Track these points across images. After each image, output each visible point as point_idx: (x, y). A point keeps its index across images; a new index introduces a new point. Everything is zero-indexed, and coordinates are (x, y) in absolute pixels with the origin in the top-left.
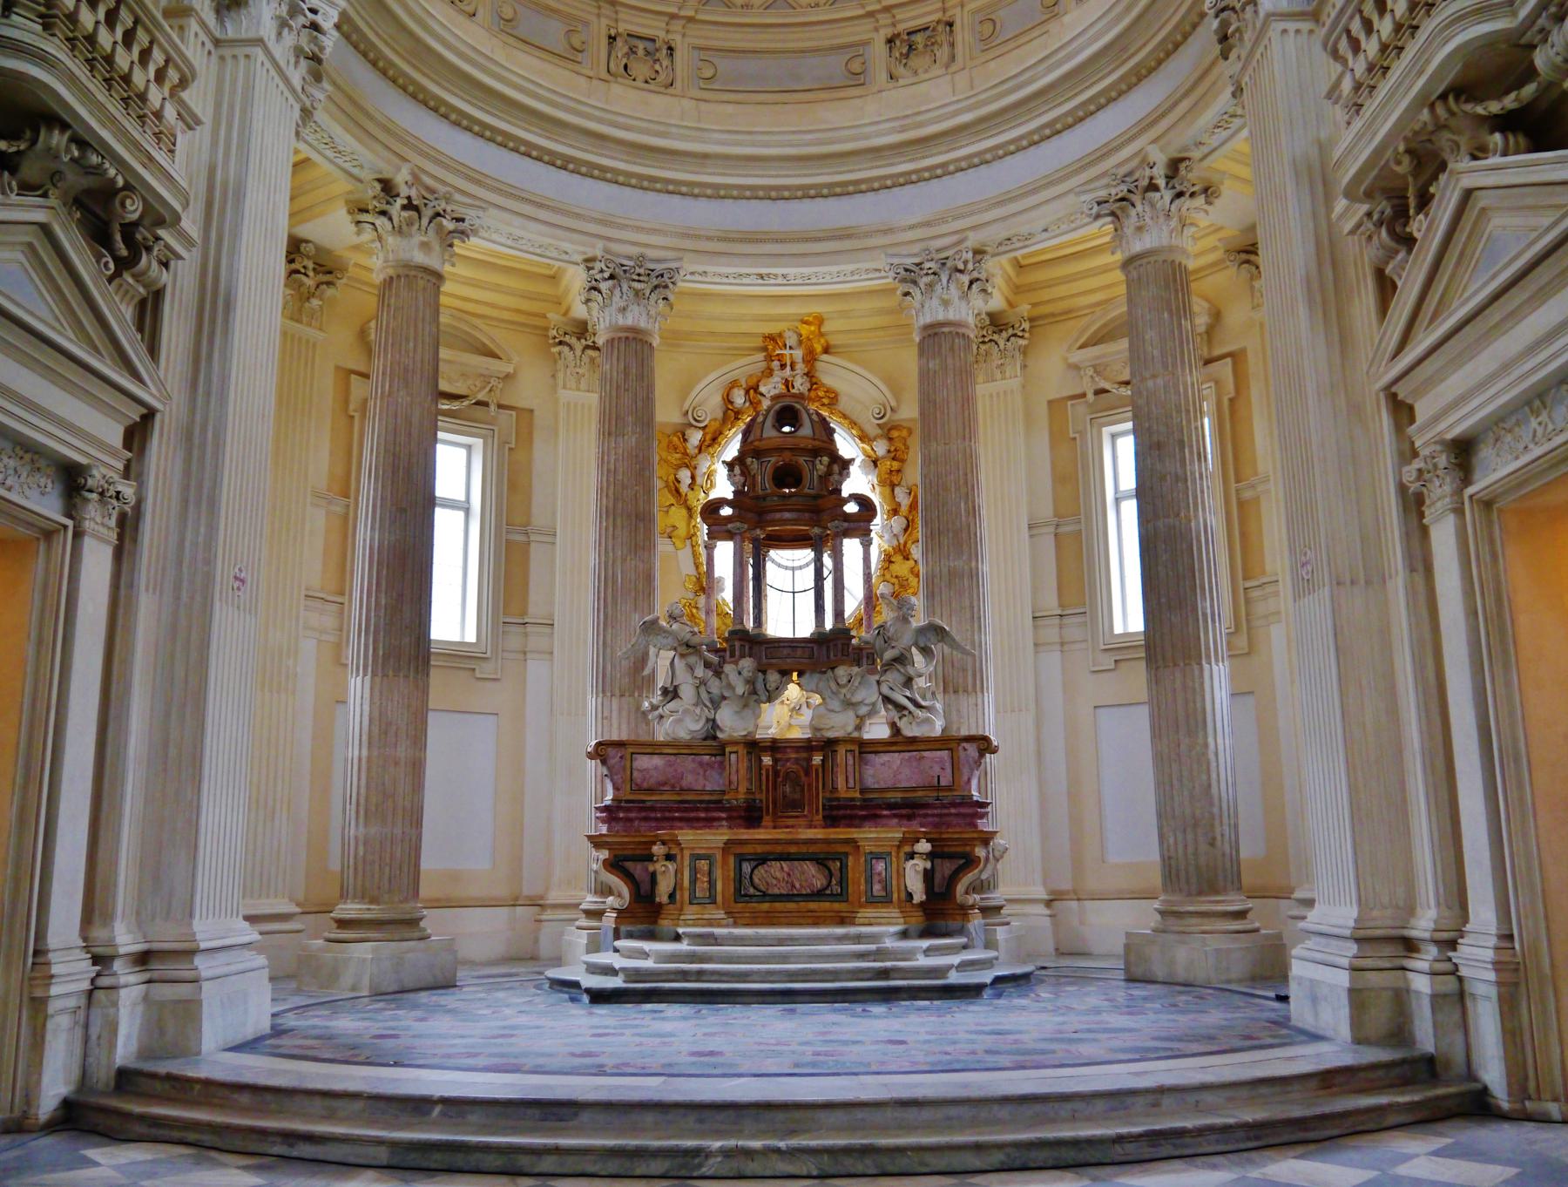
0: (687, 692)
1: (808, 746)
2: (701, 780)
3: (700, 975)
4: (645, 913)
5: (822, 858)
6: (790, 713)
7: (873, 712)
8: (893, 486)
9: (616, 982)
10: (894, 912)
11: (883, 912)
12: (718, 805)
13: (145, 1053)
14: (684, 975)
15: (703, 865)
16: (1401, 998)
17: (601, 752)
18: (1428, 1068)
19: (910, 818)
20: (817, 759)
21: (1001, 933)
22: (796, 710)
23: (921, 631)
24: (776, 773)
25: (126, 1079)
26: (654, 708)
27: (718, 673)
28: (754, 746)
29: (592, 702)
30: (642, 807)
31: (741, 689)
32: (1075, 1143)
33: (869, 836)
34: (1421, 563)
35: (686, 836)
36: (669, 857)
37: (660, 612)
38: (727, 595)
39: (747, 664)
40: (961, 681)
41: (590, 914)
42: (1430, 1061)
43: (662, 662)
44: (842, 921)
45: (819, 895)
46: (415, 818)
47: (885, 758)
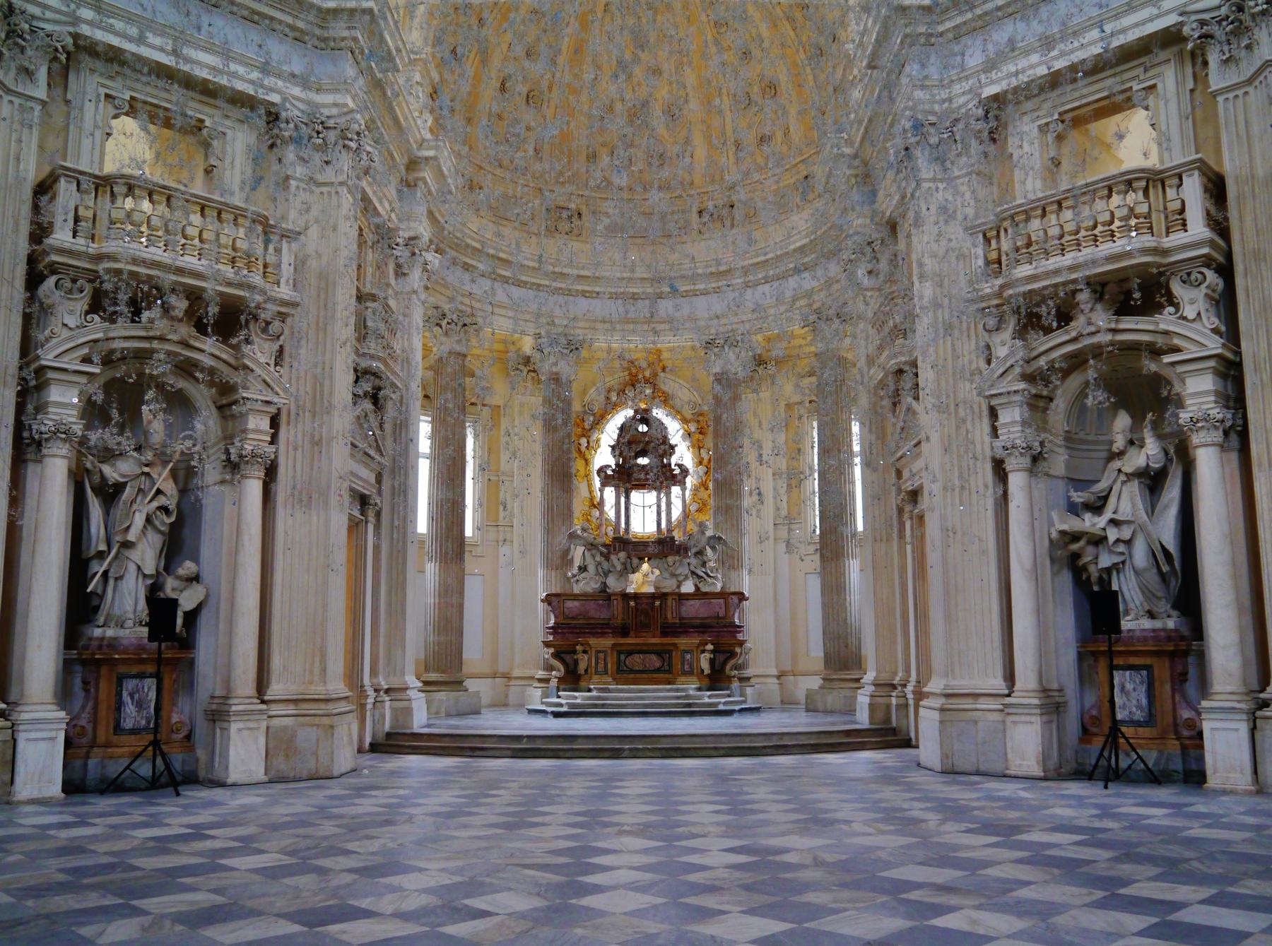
0: (591, 568)
1: (652, 597)
2: (599, 613)
3: (603, 706)
4: (572, 679)
5: (661, 652)
6: (644, 579)
7: (686, 578)
8: (699, 448)
9: (564, 709)
10: (695, 679)
11: (690, 679)
12: (607, 625)
13: (391, 727)
14: (596, 706)
15: (602, 655)
16: (888, 706)
17: (548, 599)
18: (894, 731)
19: (704, 633)
20: (657, 603)
21: (749, 691)
22: (646, 575)
23: (710, 538)
24: (637, 610)
25: (389, 735)
26: (574, 576)
27: (607, 558)
28: (625, 596)
29: (540, 573)
30: (571, 628)
31: (619, 567)
32: (749, 748)
33: (683, 642)
34: (901, 535)
35: (593, 641)
36: (585, 652)
37: (577, 527)
38: (611, 514)
39: (622, 555)
40: (732, 560)
41: (540, 680)
42: (894, 729)
43: (578, 553)
44: (669, 683)
45: (658, 670)
46: (460, 632)
47: (692, 602)
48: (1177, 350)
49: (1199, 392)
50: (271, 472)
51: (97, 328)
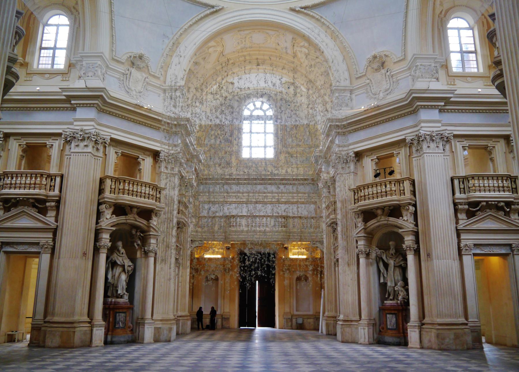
48: (401, 228)
49: (409, 240)
50: (156, 254)
51: (115, 219)
